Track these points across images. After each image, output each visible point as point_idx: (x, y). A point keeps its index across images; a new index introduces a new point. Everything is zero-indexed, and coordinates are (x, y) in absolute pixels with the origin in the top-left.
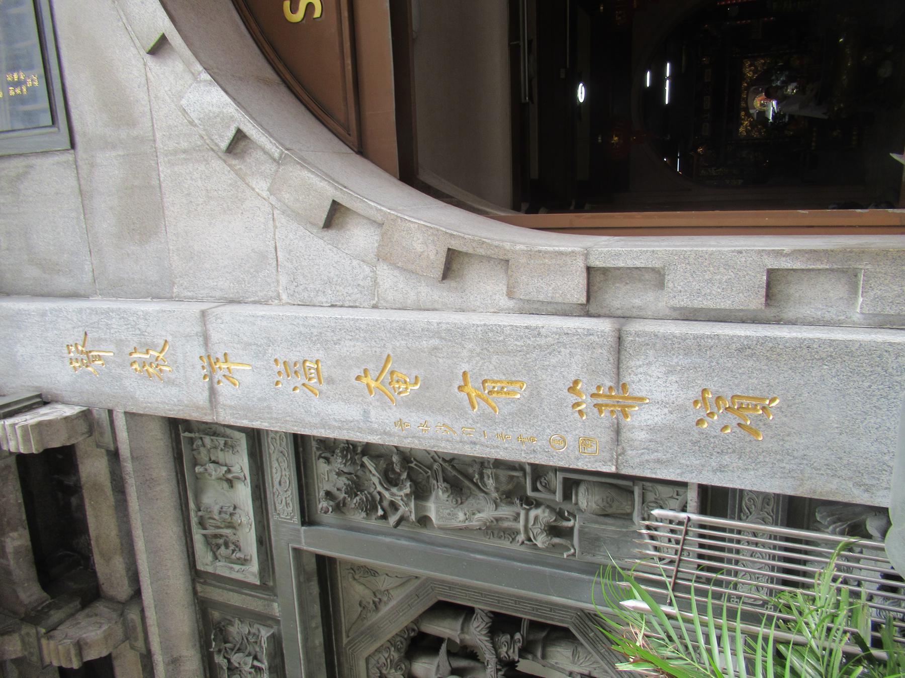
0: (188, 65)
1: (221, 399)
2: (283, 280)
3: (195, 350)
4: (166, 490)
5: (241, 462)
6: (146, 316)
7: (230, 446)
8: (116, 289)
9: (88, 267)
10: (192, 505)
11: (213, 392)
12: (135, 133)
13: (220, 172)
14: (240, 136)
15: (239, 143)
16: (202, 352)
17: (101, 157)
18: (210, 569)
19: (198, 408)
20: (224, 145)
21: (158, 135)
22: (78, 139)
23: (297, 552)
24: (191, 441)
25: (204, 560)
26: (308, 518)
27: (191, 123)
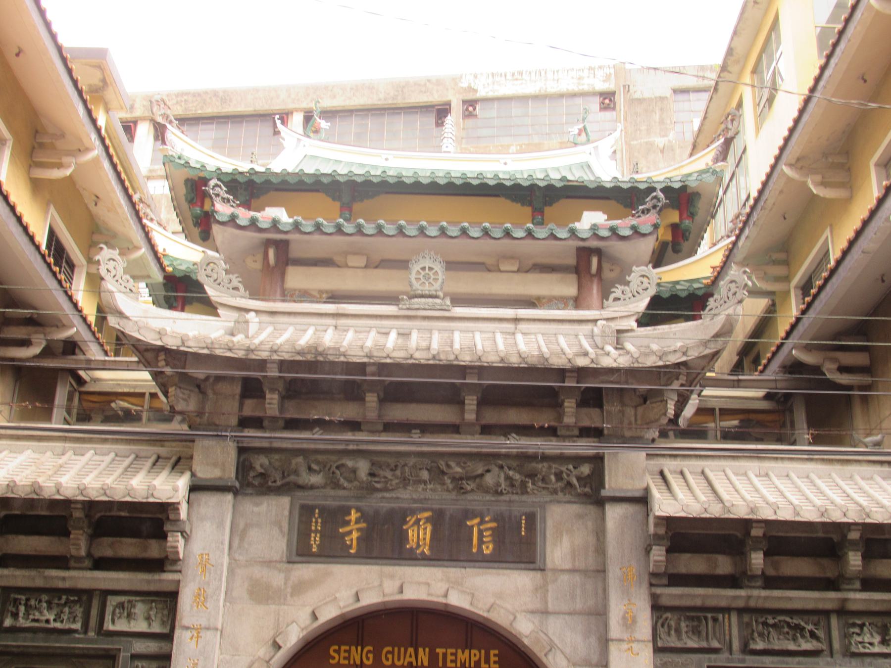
0: (306, 628)
1: (184, 632)
2: (228, 657)
3: (204, 622)
4: (145, 588)
5: (156, 628)
6: (218, 600)
7: (163, 623)
8: (231, 571)
9: (241, 558)
10: (138, 598)
11: (187, 628)
12: (288, 596)
13: (268, 634)
14: (280, 647)
15: (277, 646)
16: (203, 626)
17: (282, 575)
18: (108, 603)
19: (181, 619)
20: (278, 640)
21: (286, 607)
22: (291, 565)
23: (120, 650)
24: (165, 602)
25: (112, 601)
26: (134, 657)
27: (288, 626)
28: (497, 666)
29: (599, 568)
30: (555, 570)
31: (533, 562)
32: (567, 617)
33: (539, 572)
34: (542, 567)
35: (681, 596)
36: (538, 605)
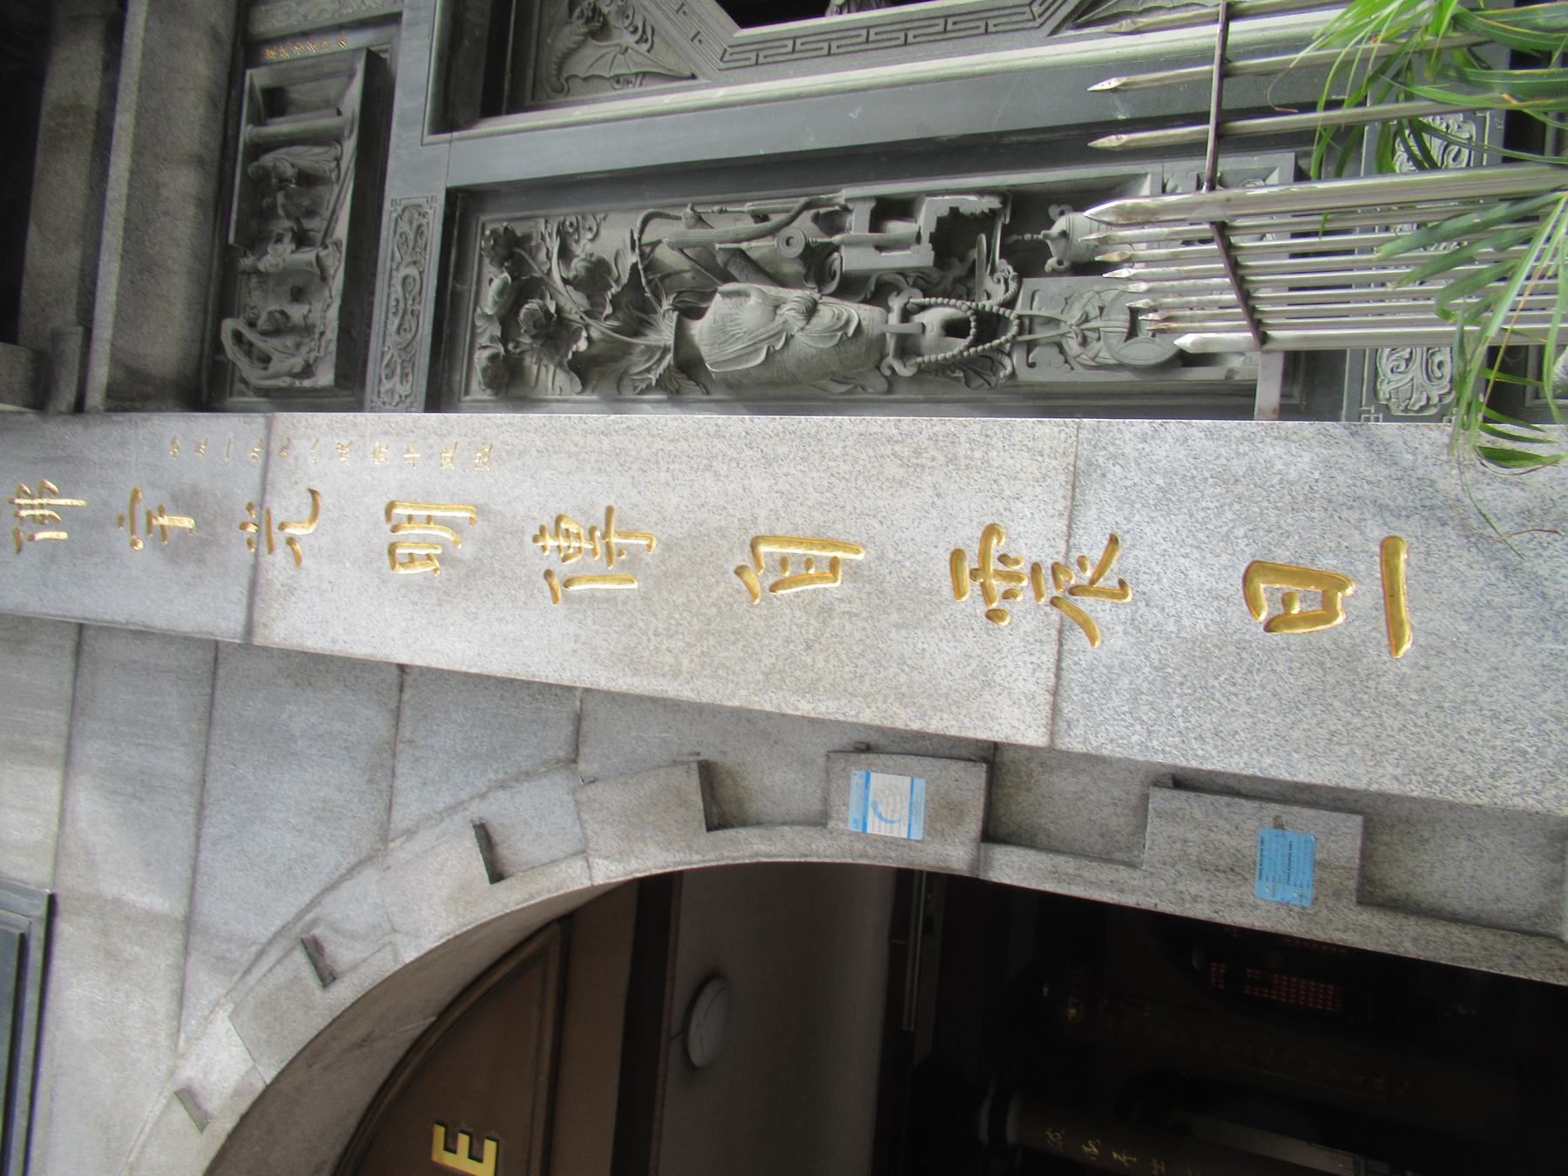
28: (490, 1147)
29: (69, 645)
30: (59, 854)
31: (23, 942)
32: (210, 831)
33: (63, 927)
34: (41, 911)
35: (140, 265)
36: (159, 960)
